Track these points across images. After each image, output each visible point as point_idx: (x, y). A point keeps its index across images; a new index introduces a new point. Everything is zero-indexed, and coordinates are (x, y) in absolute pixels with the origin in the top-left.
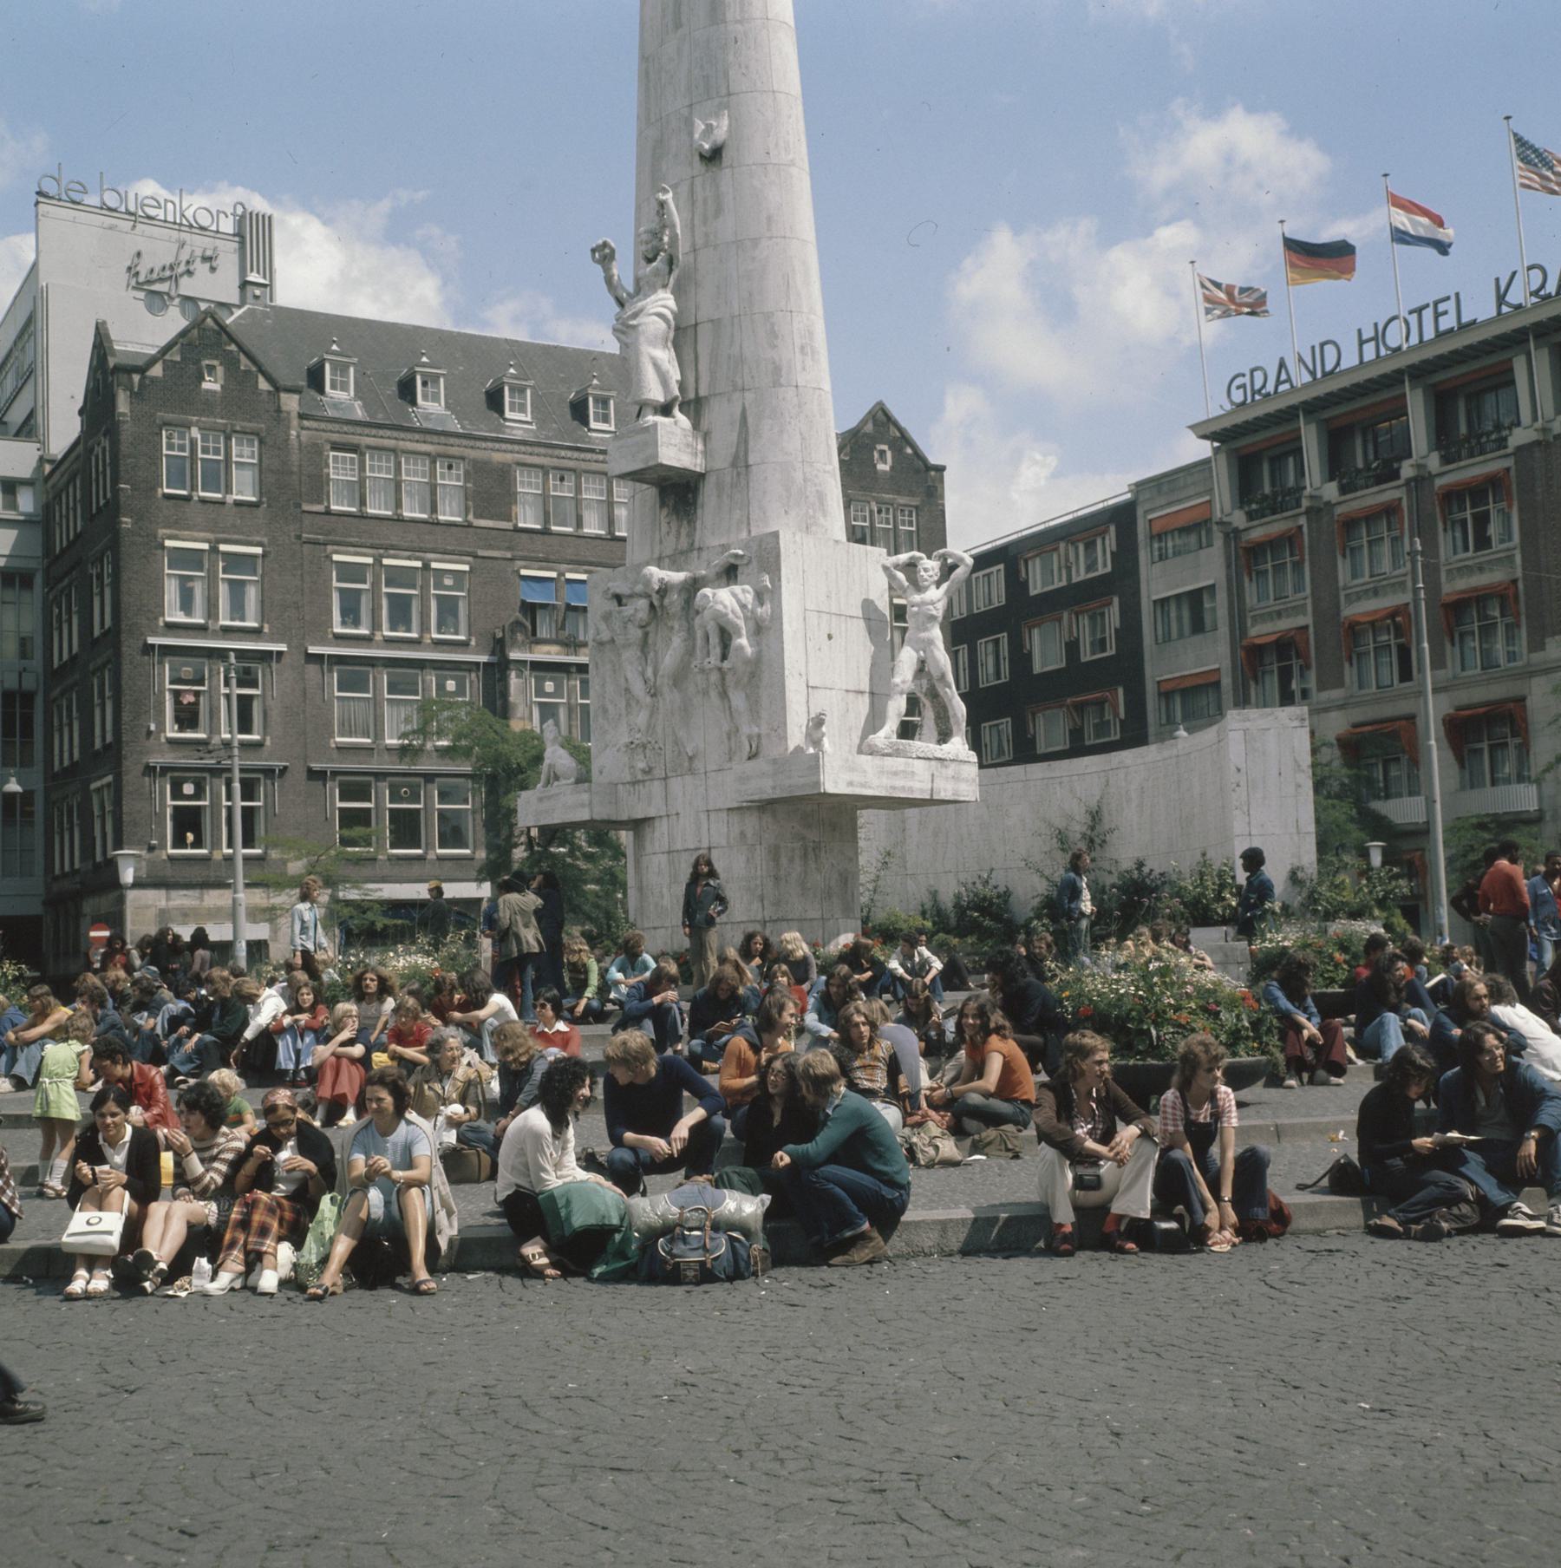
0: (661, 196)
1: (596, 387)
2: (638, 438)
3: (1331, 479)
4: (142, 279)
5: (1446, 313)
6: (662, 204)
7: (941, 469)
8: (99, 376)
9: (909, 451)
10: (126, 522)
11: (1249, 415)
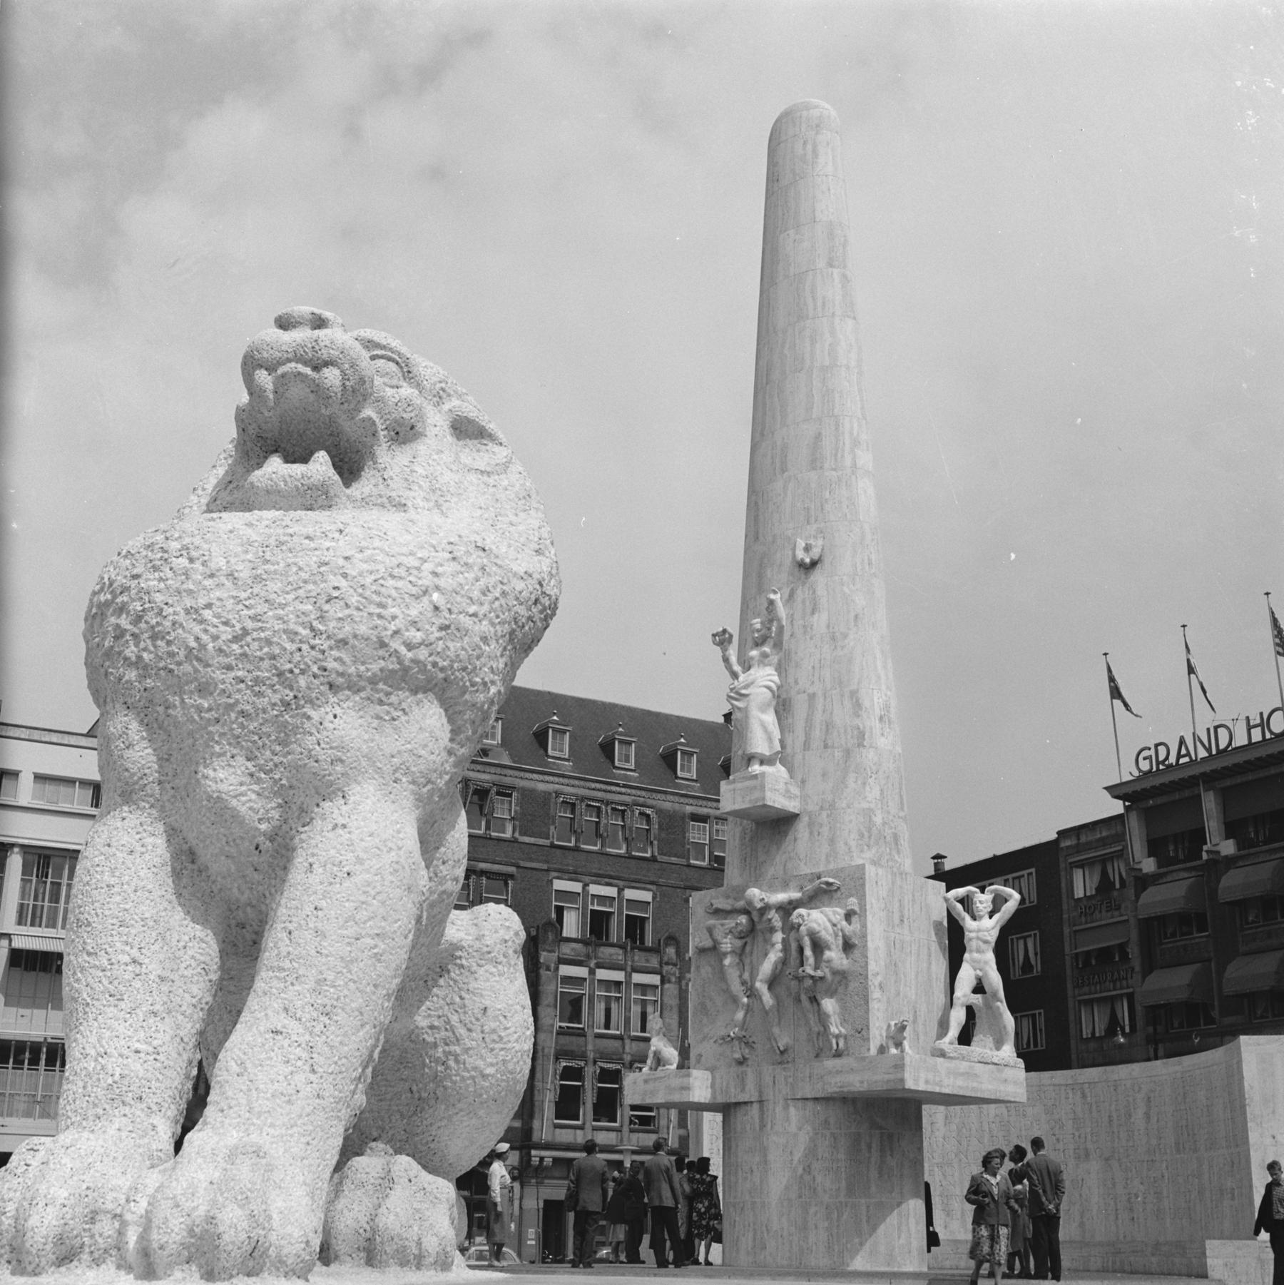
0: (772, 596)
1: (621, 734)
2: (749, 783)
3: (1227, 838)
6: (771, 602)
11: (1157, 781)
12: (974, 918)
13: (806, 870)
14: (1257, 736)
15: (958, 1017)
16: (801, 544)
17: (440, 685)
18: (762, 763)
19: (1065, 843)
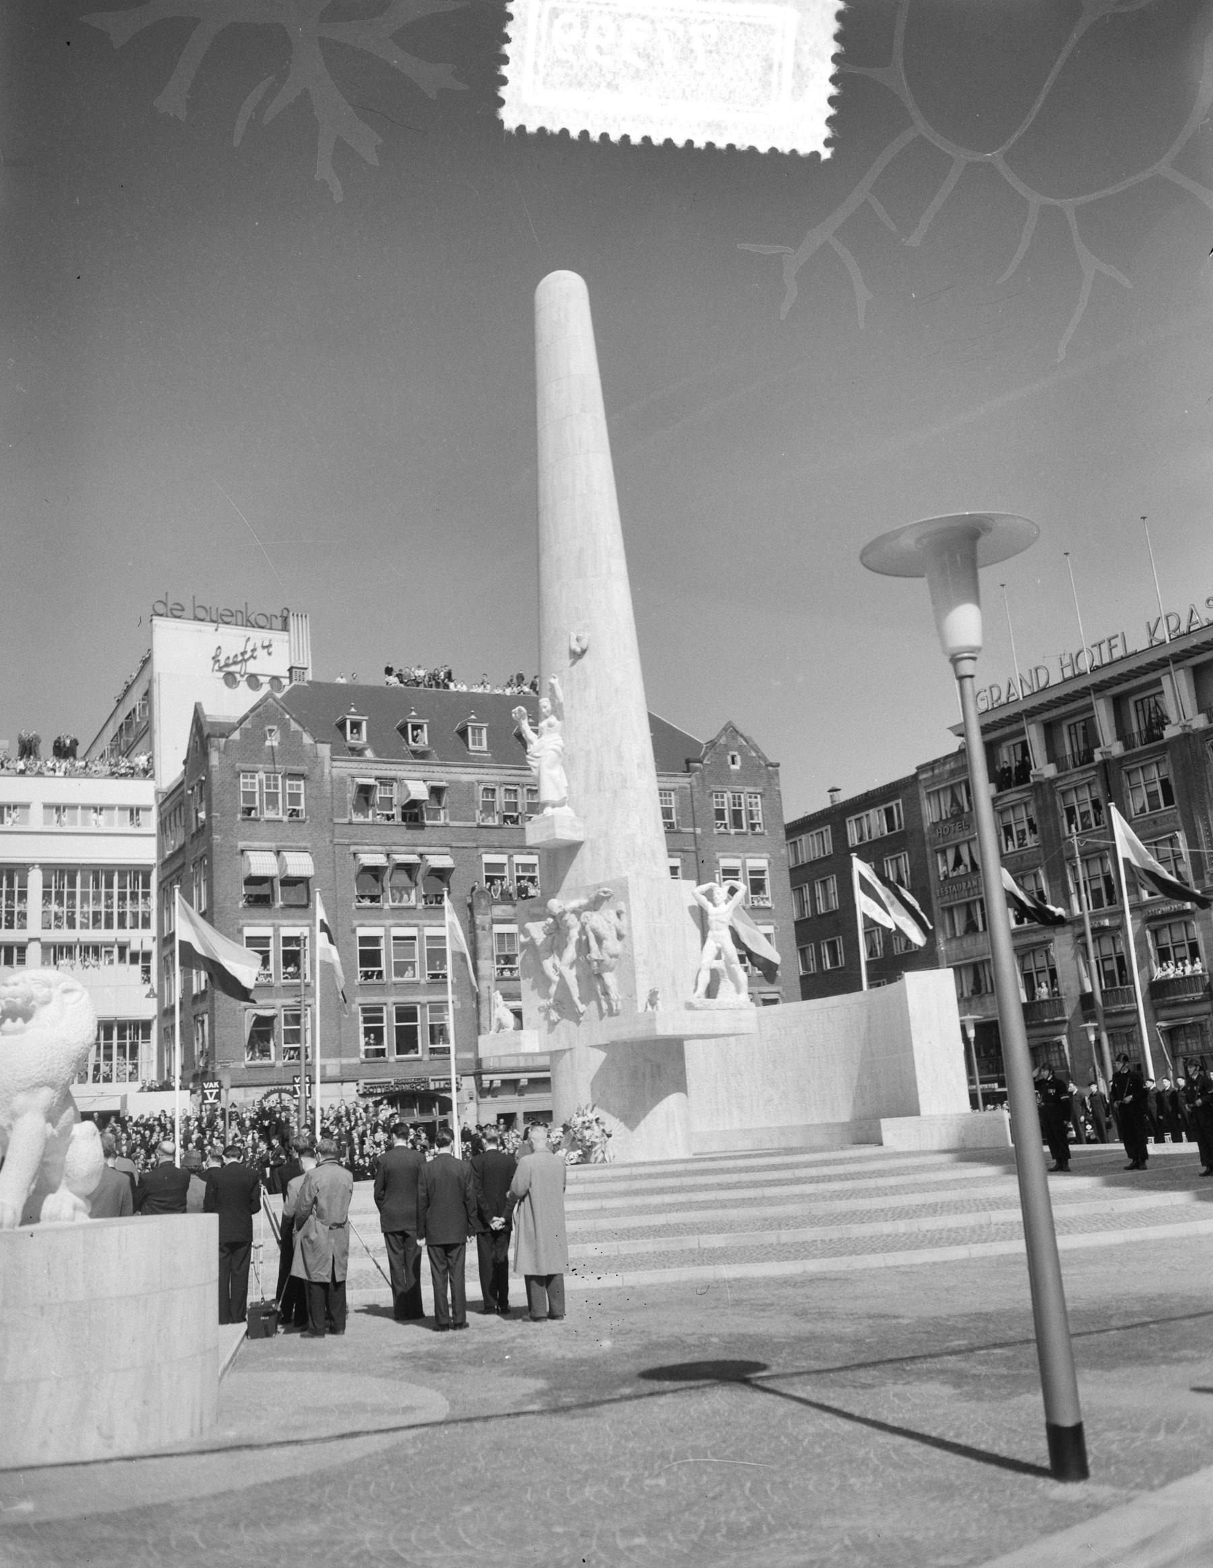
0: (552, 681)
4: (222, 663)
5: (1116, 646)
7: (778, 765)
8: (197, 739)
9: (754, 754)
10: (217, 838)
12: (715, 905)
13: (590, 882)
14: (1068, 673)
15: (705, 979)
16: (574, 636)
17: (52, 1085)
18: (554, 806)
19: (922, 777)
